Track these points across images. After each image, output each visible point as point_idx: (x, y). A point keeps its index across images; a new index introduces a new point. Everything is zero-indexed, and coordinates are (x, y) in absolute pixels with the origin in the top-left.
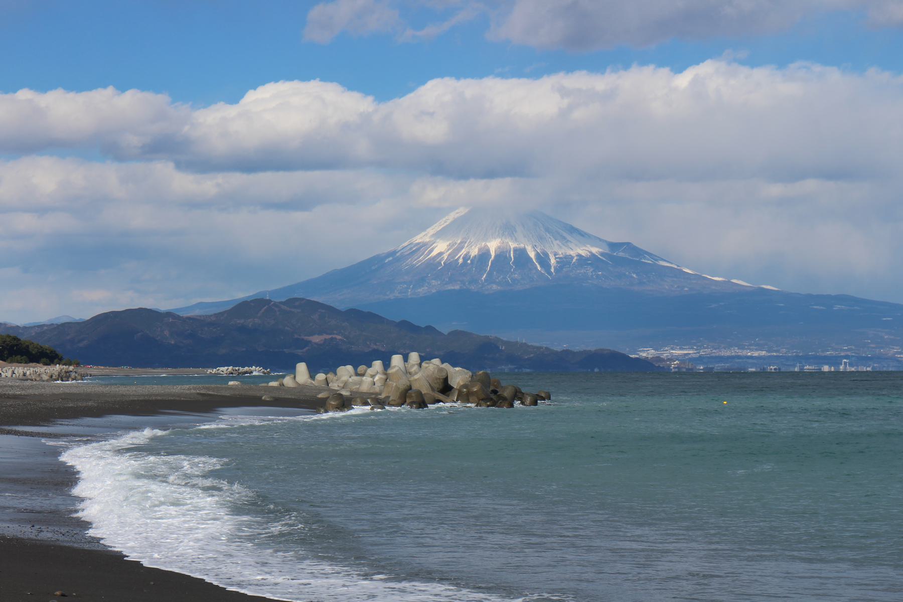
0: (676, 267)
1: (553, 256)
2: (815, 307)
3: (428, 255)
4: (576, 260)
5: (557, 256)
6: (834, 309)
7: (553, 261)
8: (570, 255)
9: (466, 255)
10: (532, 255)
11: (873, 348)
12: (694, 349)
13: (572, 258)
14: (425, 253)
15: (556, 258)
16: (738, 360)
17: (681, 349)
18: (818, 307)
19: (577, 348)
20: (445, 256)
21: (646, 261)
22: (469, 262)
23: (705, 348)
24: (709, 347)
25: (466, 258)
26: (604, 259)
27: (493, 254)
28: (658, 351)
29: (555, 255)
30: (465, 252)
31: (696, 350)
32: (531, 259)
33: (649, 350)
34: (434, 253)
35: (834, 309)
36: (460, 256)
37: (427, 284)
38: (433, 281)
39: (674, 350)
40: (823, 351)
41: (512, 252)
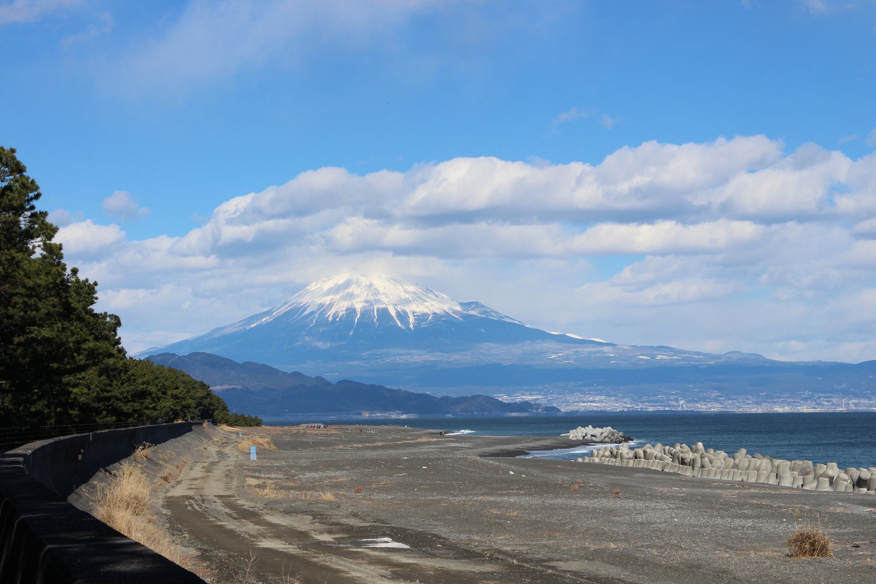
0: (518, 323)
1: (412, 314)
2: (640, 357)
3: (302, 314)
4: (432, 317)
5: (415, 314)
6: (657, 358)
7: (412, 319)
8: (427, 313)
9: (335, 313)
10: (393, 313)
11: (696, 392)
12: (541, 394)
13: (429, 315)
14: (299, 312)
15: (414, 316)
16: (583, 404)
17: (531, 395)
18: (643, 357)
19: (439, 395)
21: (493, 318)
22: (338, 319)
23: (551, 394)
24: (555, 393)
25: (335, 316)
26: (456, 316)
28: (511, 397)
29: (413, 313)
30: (334, 312)
31: (544, 395)
32: (392, 317)
33: (502, 396)
35: (657, 358)
36: (330, 314)
37: (300, 340)
38: (306, 337)
39: (524, 396)
40: (654, 396)
41: (375, 311)
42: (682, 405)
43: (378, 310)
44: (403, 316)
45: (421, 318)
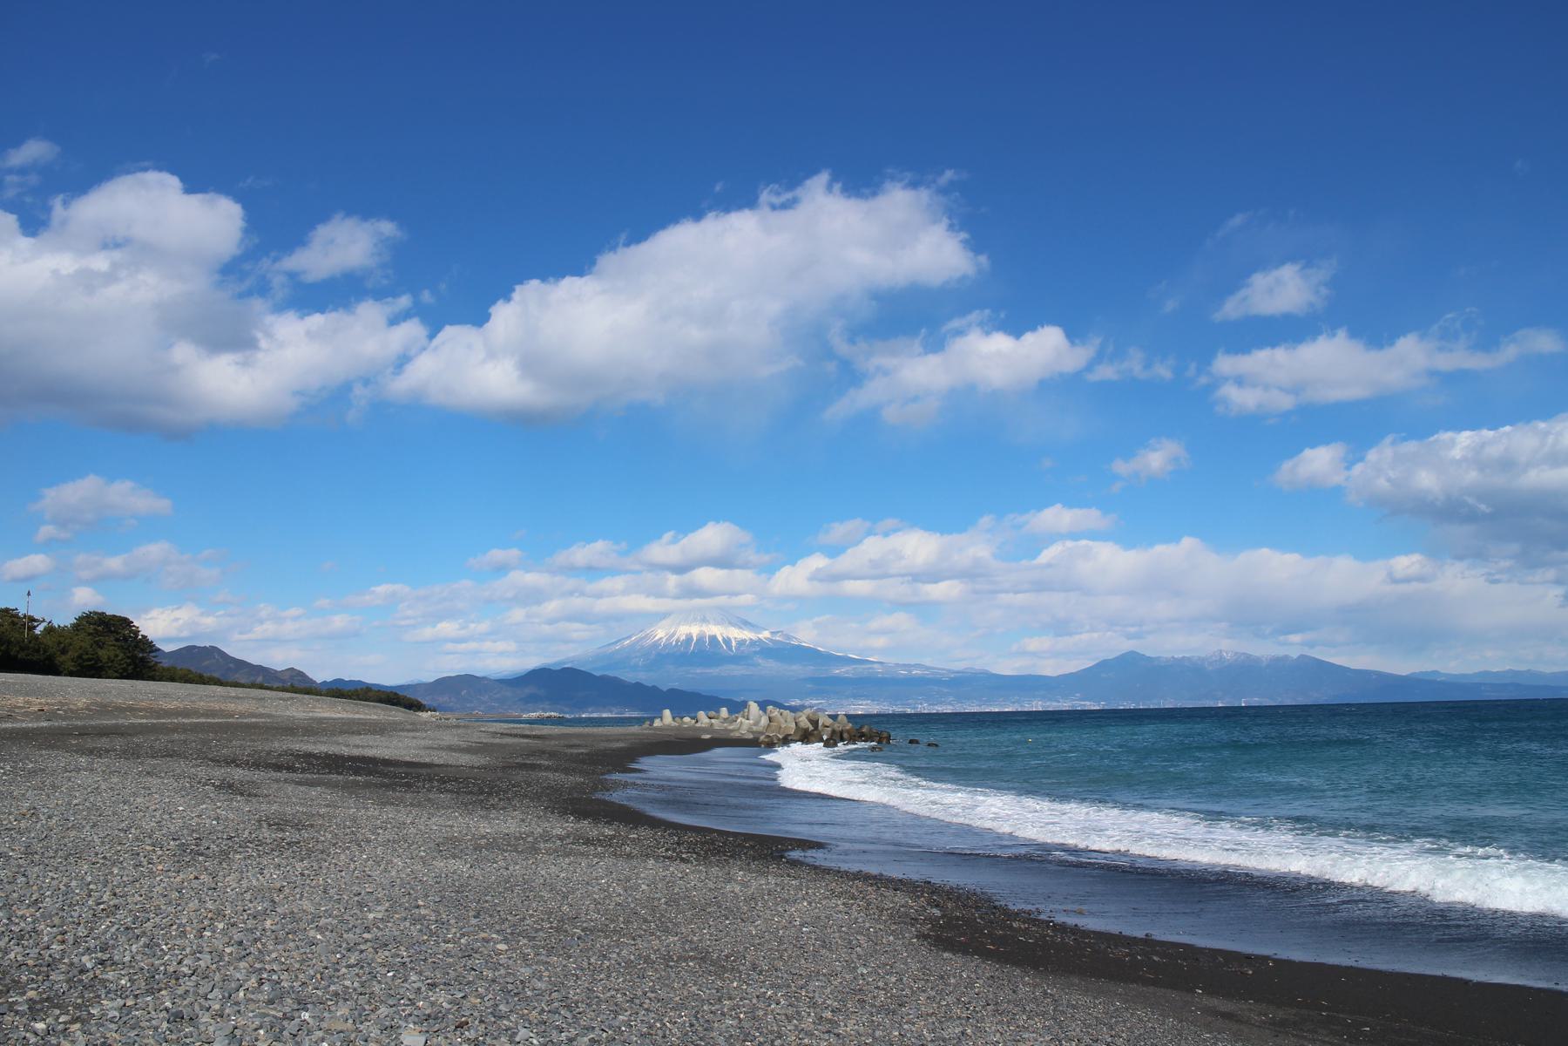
7: (734, 644)
10: (720, 639)
20: (664, 640)
25: (677, 641)
27: (695, 639)
34: (657, 638)
42: (925, 708)
43: (709, 636)
44: (727, 641)
45: (741, 643)
